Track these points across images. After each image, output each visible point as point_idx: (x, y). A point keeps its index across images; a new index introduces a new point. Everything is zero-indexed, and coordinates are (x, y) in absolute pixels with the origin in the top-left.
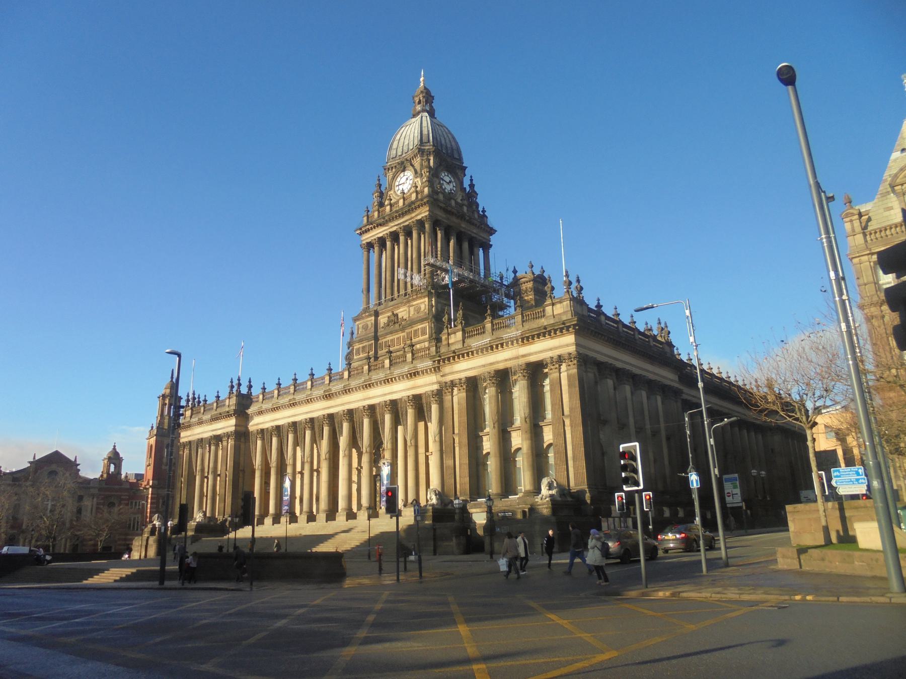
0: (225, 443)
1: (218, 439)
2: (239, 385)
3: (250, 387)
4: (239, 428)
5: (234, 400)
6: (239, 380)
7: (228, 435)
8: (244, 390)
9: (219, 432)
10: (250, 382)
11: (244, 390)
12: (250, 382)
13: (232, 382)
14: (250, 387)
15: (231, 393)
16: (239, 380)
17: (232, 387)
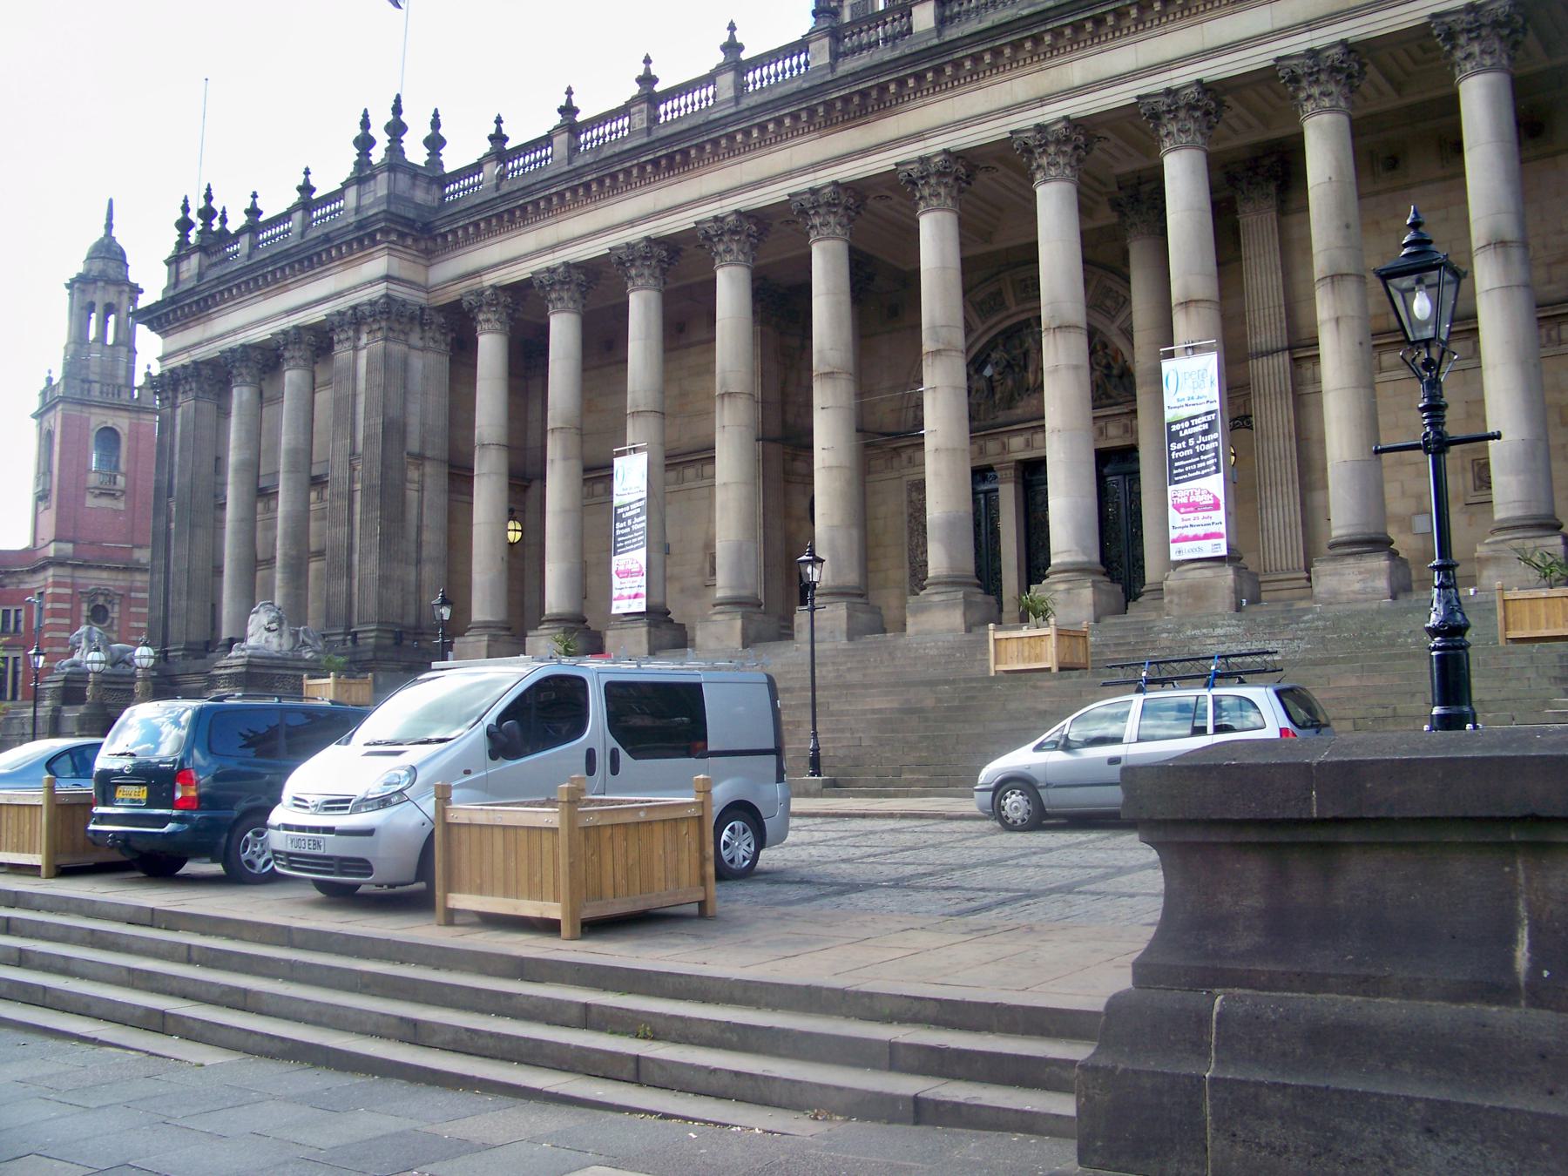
0: (342, 353)
1: (318, 342)
2: (397, 129)
3: (435, 143)
4: (400, 292)
5: (380, 187)
6: (397, 109)
7: (356, 319)
8: (416, 153)
9: (317, 315)
10: (436, 124)
11: (416, 153)
12: (436, 124)
13: (365, 124)
14: (435, 143)
15: (363, 162)
16: (397, 109)
17: (364, 143)
